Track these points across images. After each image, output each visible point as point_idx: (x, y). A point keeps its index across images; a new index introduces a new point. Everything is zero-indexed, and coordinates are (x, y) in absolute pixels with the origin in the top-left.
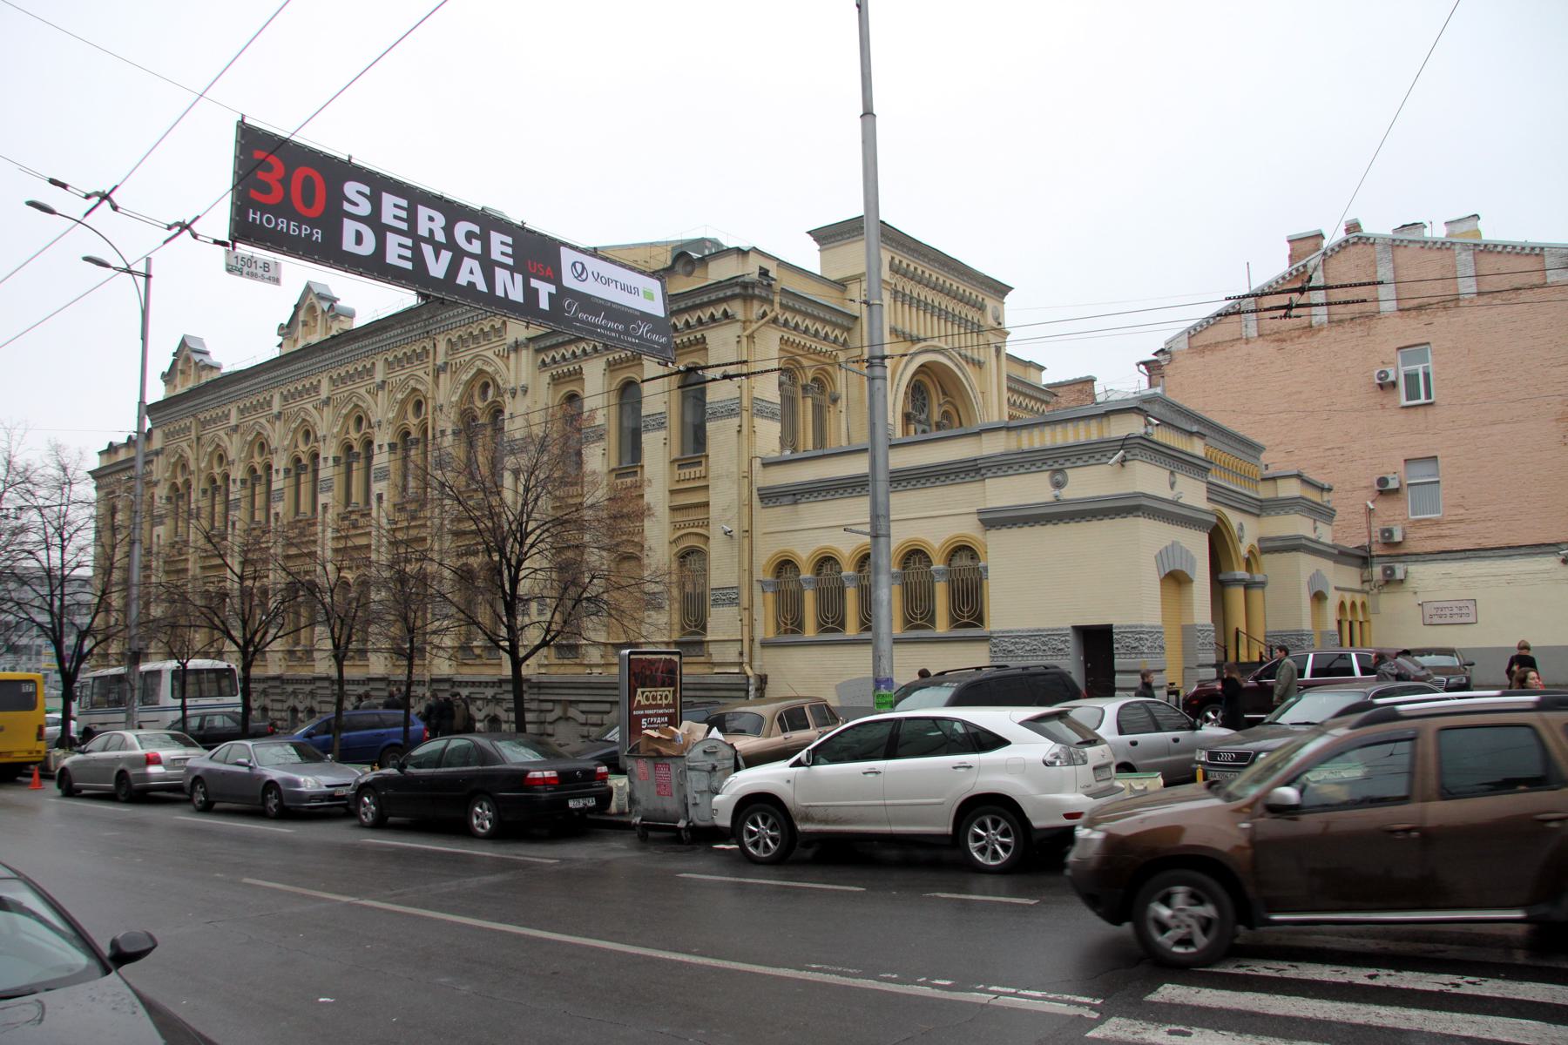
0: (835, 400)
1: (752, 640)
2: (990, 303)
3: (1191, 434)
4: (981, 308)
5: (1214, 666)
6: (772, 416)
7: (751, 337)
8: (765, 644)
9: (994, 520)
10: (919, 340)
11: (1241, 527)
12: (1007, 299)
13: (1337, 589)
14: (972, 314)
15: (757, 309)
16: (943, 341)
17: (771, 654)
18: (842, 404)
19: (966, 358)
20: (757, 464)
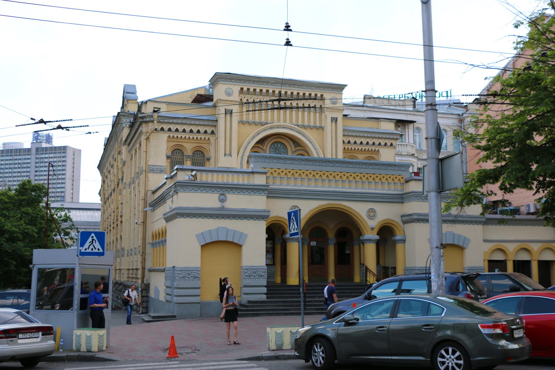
0: (208, 160)
1: (144, 269)
2: (328, 96)
3: (253, 173)
4: (322, 98)
5: (265, 286)
6: (161, 171)
7: (148, 139)
8: (150, 271)
9: (169, 218)
10: (267, 124)
11: (372, 210)
12: (344, 91)
13: (485, 241)
14: (318, 103)
15: (151, 126)
16: (283, 122)
17: (153, 274)
18: (212, 160)
19: (304, 127)
20: (149, 193)
